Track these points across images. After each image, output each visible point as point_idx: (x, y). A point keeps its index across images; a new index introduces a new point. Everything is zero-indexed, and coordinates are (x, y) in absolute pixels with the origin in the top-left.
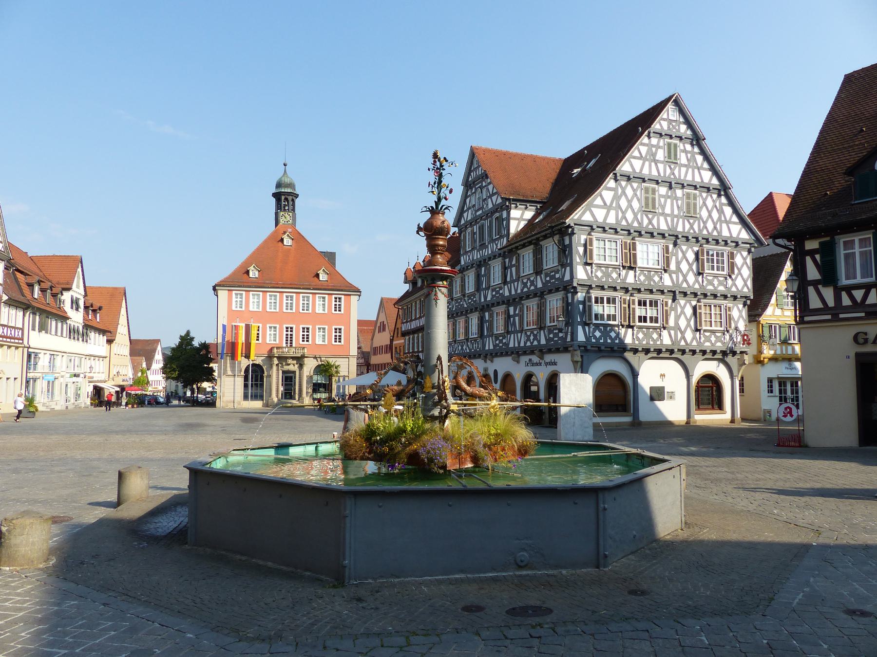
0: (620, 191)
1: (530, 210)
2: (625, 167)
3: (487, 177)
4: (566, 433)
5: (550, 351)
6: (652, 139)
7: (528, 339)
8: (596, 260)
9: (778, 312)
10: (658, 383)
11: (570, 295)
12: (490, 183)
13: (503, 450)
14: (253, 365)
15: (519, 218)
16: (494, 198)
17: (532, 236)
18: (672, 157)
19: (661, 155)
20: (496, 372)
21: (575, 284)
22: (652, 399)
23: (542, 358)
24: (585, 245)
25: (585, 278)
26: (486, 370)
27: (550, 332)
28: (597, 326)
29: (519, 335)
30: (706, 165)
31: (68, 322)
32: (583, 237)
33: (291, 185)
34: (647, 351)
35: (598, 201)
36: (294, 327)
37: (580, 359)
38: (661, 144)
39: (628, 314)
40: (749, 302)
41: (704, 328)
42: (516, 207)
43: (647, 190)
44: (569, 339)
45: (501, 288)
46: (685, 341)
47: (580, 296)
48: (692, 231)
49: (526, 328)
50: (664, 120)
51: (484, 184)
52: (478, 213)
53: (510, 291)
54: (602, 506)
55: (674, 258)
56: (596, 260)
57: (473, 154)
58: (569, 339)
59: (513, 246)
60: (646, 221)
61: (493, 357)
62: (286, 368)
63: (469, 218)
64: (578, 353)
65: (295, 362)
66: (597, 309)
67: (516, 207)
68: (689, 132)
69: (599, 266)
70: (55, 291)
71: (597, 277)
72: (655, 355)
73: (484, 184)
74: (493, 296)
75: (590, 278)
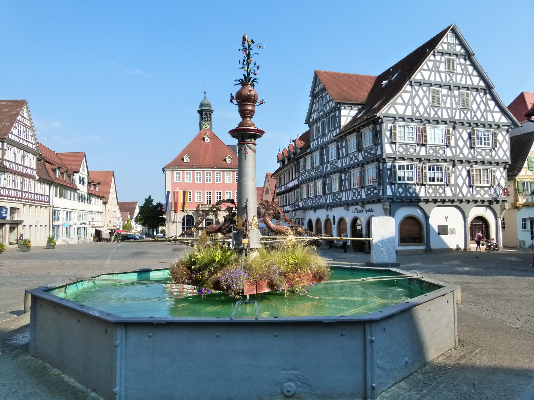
0: (414, 93)
1: (354, 110)
2: (417, 76)
3: (325, 90)
4: (376, 257)
5: (368, 203)
6: (436, 56)
7: (354, 195)
8: (399, 141)
9: (529, 173)
10: (443, 223)
11: (381, 164)
12: (327, 94)
13: (300, 277)
14: (187, 216)
15: (347, 115)
16: (330, 103)
17: (355, 127)
18: (450, 66)
19: (442, 67)
20: (334, 217)
21: (384, 157)
22: (439, 234)
23: (363, 207)
24: (391, 131)
25: (392, 152)
26: (328, 216)
27: (368, 189)
28: (400, 185)
29: (348, 192)
30: (475, 73)
31: (78, 191)
32: (389, 125)
33: (209, 105)
34: (435, 201)
35: (399, 100)
36: (212, 192)
37: (388, 207)
38: (443, 59)
39: (422, 176)
40: (508, 166)
41: (476, 185)
42: (345, 108)
43: (433, 91)
44: (381, 194)
45: (336, 162)
46: (462, 194)
47: (389, 164)
48: (466, 119)
49: (352, 187)
50: (445, 43)
51: (324, 95)
52: (320, 114)
53: (342, 164)
54: (369, 338)
55: (453, 137)
56: (398, 140)
57: (316, 76)
58: (381, 194)
59: (343, 134)
60: (433, 113)
61: (332, 207)
62: (208, 217)
63: (315, 118)
64: (388, 203)
65: (212, 213)
66: (400, 173)
67: (345, 108)
68: (463, 51)
69: (401, 144)
70: (69, 173)
71: (399, 151)
72: (441, 204)
73: (324, 95)
74: (331, 168)
75: (395, 153)
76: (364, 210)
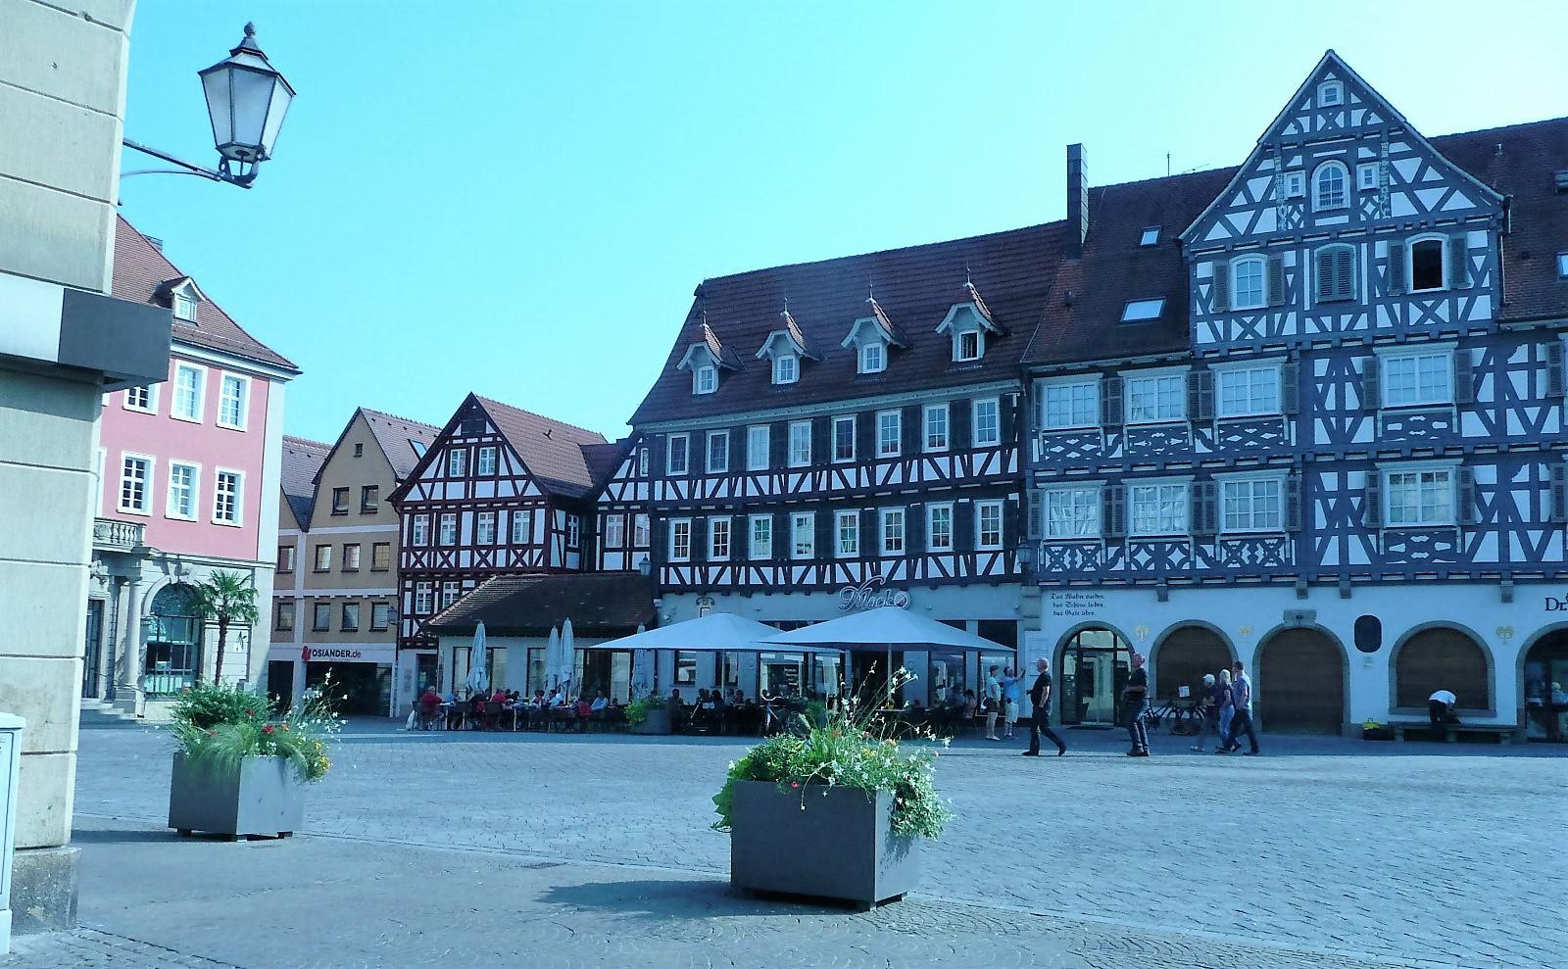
29: (1535, 536)
52: (1319, 222)
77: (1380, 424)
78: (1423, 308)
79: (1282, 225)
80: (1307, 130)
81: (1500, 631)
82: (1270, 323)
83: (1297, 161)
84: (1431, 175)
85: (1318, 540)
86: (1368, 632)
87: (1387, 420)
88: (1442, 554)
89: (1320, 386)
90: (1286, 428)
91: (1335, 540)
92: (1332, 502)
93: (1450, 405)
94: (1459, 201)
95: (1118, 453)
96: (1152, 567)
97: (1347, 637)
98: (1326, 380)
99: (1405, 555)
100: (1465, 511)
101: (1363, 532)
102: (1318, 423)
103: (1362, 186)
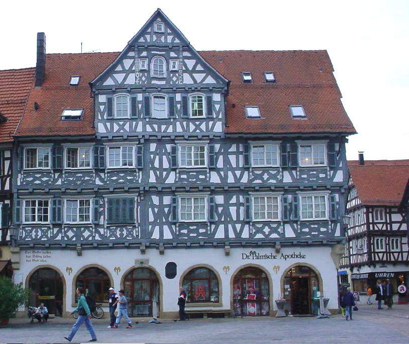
52: (153, 82)
76: (279, 256)
77: (178, 175)
78: (195, 125)
79: (137, 82)
80: (149, 41)
81: (225, 268)
82: (131, 127)
83: (144, 54)
84: (199, 68)
85: (150, 226)
86: (171, 270)
87: (180, 173)
88: (202, 234)
89: (152, 156)
90: (137, 174)
91: (157, 228)
92: (156, 210)
93: (206, 168)
94: (210, 80)
95: (59, 182)
96: (74, 239)
97: (161, 272)
98: (155, 153)
99: (187, 235)
100: (211, 216)
101: (170, 224)
102: (152, 172)
103: (171, 68)
